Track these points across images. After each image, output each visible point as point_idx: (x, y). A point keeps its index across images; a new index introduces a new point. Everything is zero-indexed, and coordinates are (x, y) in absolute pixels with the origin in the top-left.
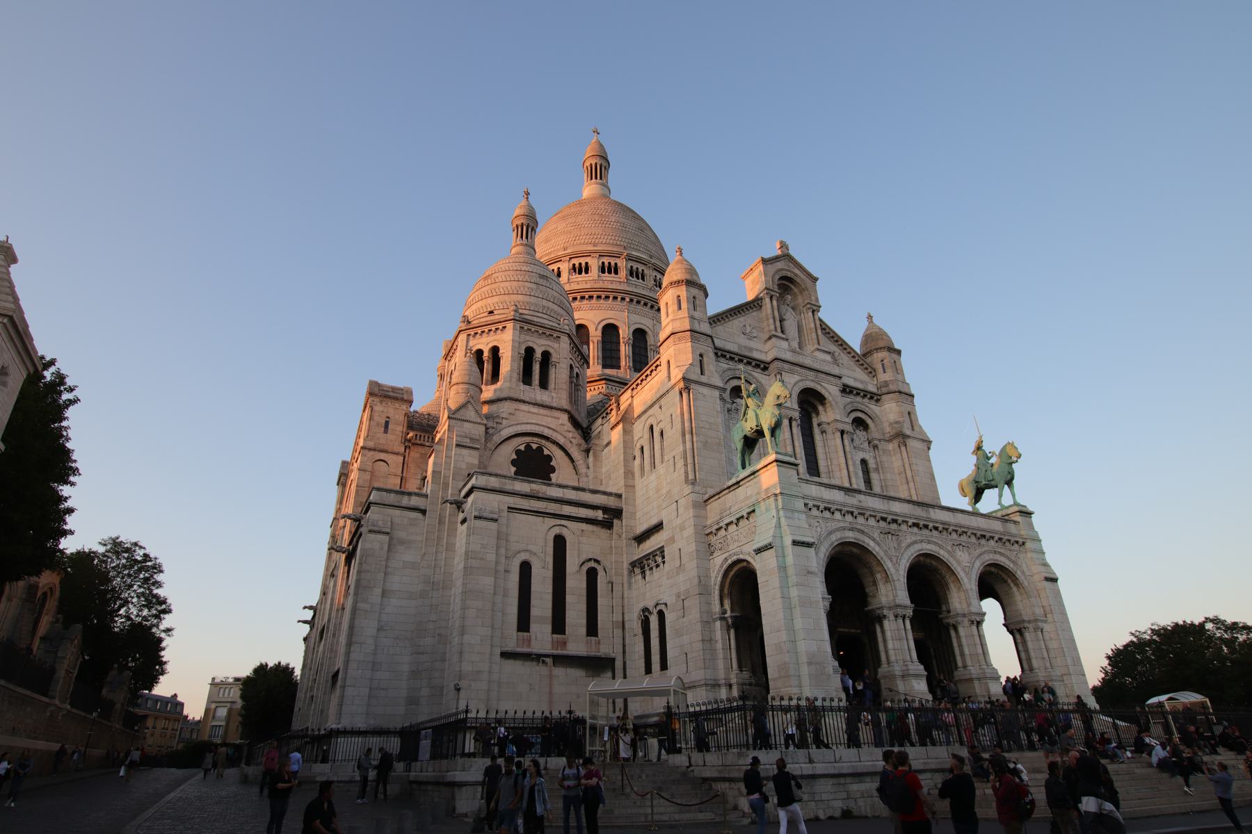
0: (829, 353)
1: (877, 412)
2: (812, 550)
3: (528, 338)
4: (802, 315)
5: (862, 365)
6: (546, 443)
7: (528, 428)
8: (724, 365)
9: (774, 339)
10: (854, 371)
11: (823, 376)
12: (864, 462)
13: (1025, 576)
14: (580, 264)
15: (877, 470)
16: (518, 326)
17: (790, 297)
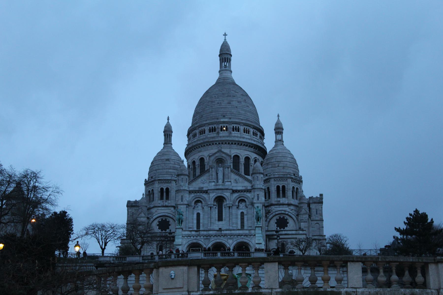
0: (231, 181)
1: (248, 195)
2: (181, 246)
3: (161, 185)
4: (225, 170)
5: (247, 180)
6: (168, 218)
7: (161, 214)
8: (193, 195)
9: (210, 183)
10: (244, 183)
11: (225, 190)
12: (242, 213)
13: (252, 244)
14: (202, 129)
15: (246, 215)
16: (157, 182)
17: (220, 165)
